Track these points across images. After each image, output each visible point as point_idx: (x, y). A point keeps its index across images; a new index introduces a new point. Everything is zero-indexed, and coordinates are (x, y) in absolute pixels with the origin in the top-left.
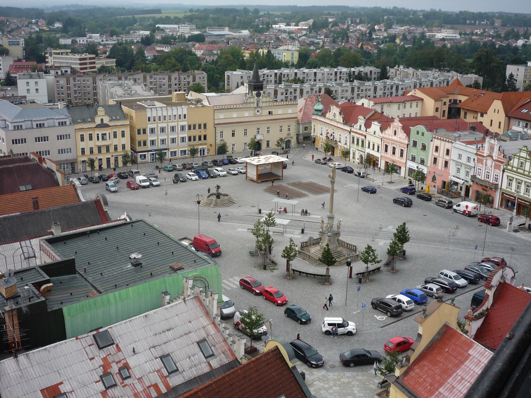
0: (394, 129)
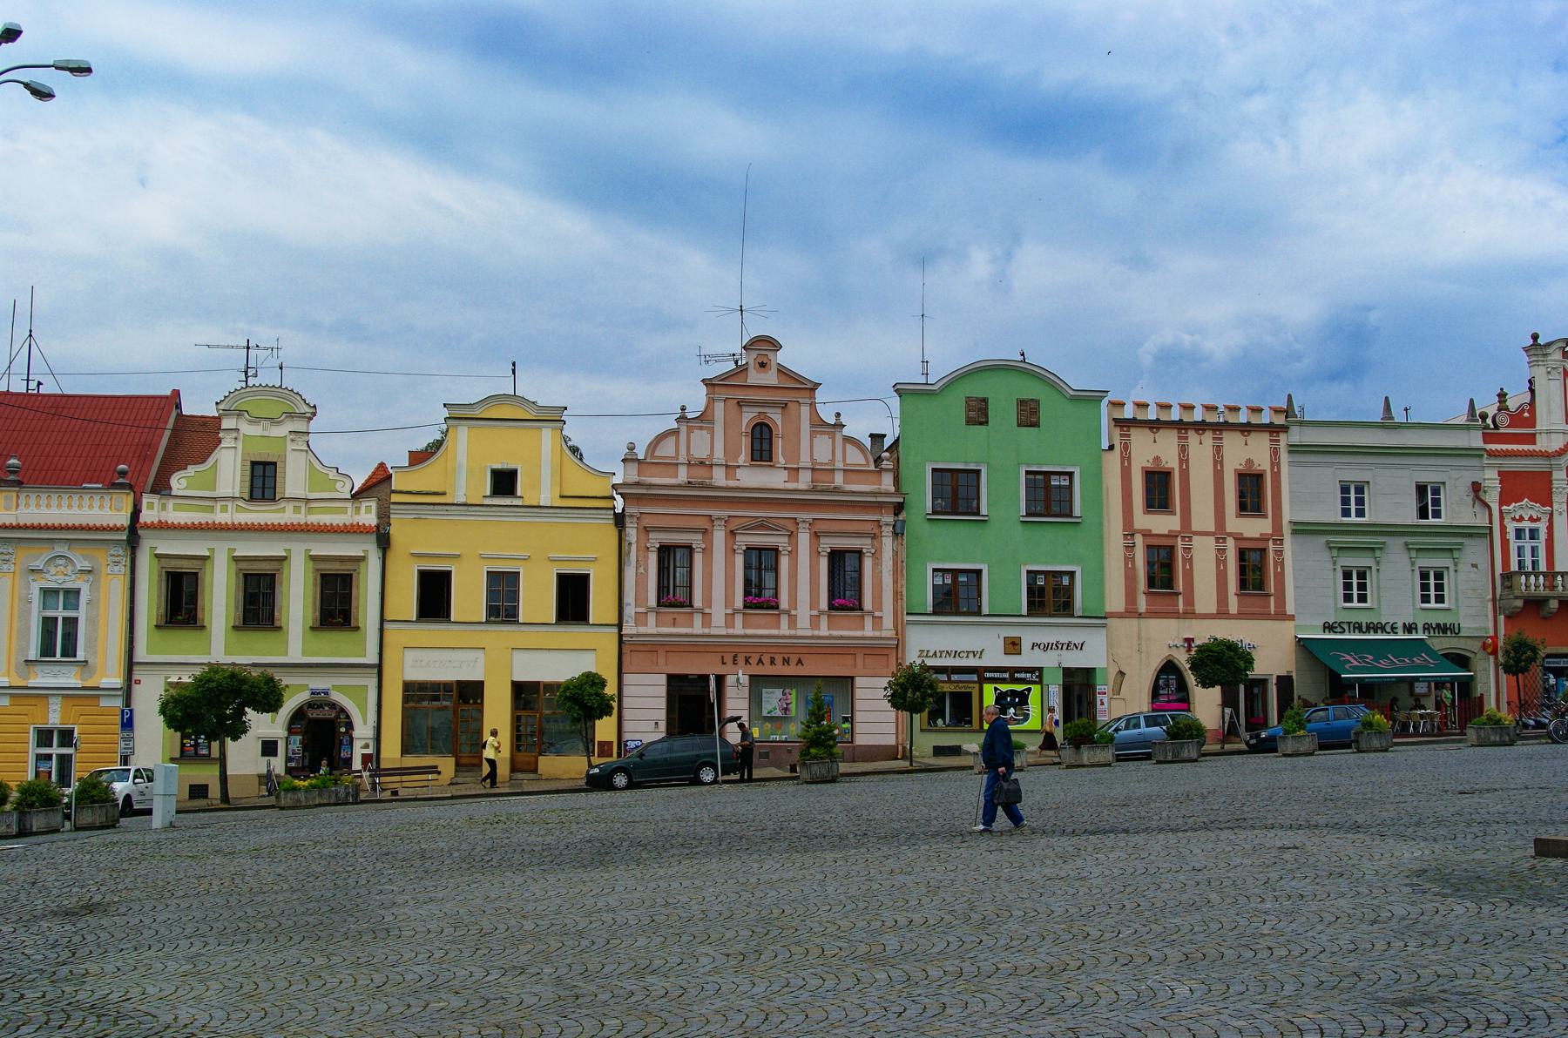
0: (749, 416)
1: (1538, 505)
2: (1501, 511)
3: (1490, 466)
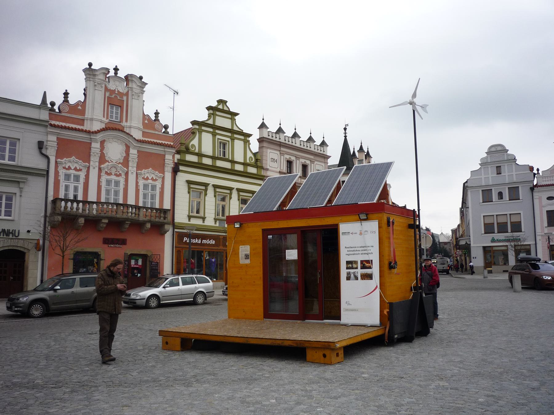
1: (81, 161)
2: (56, 162)
3: (53, 133)
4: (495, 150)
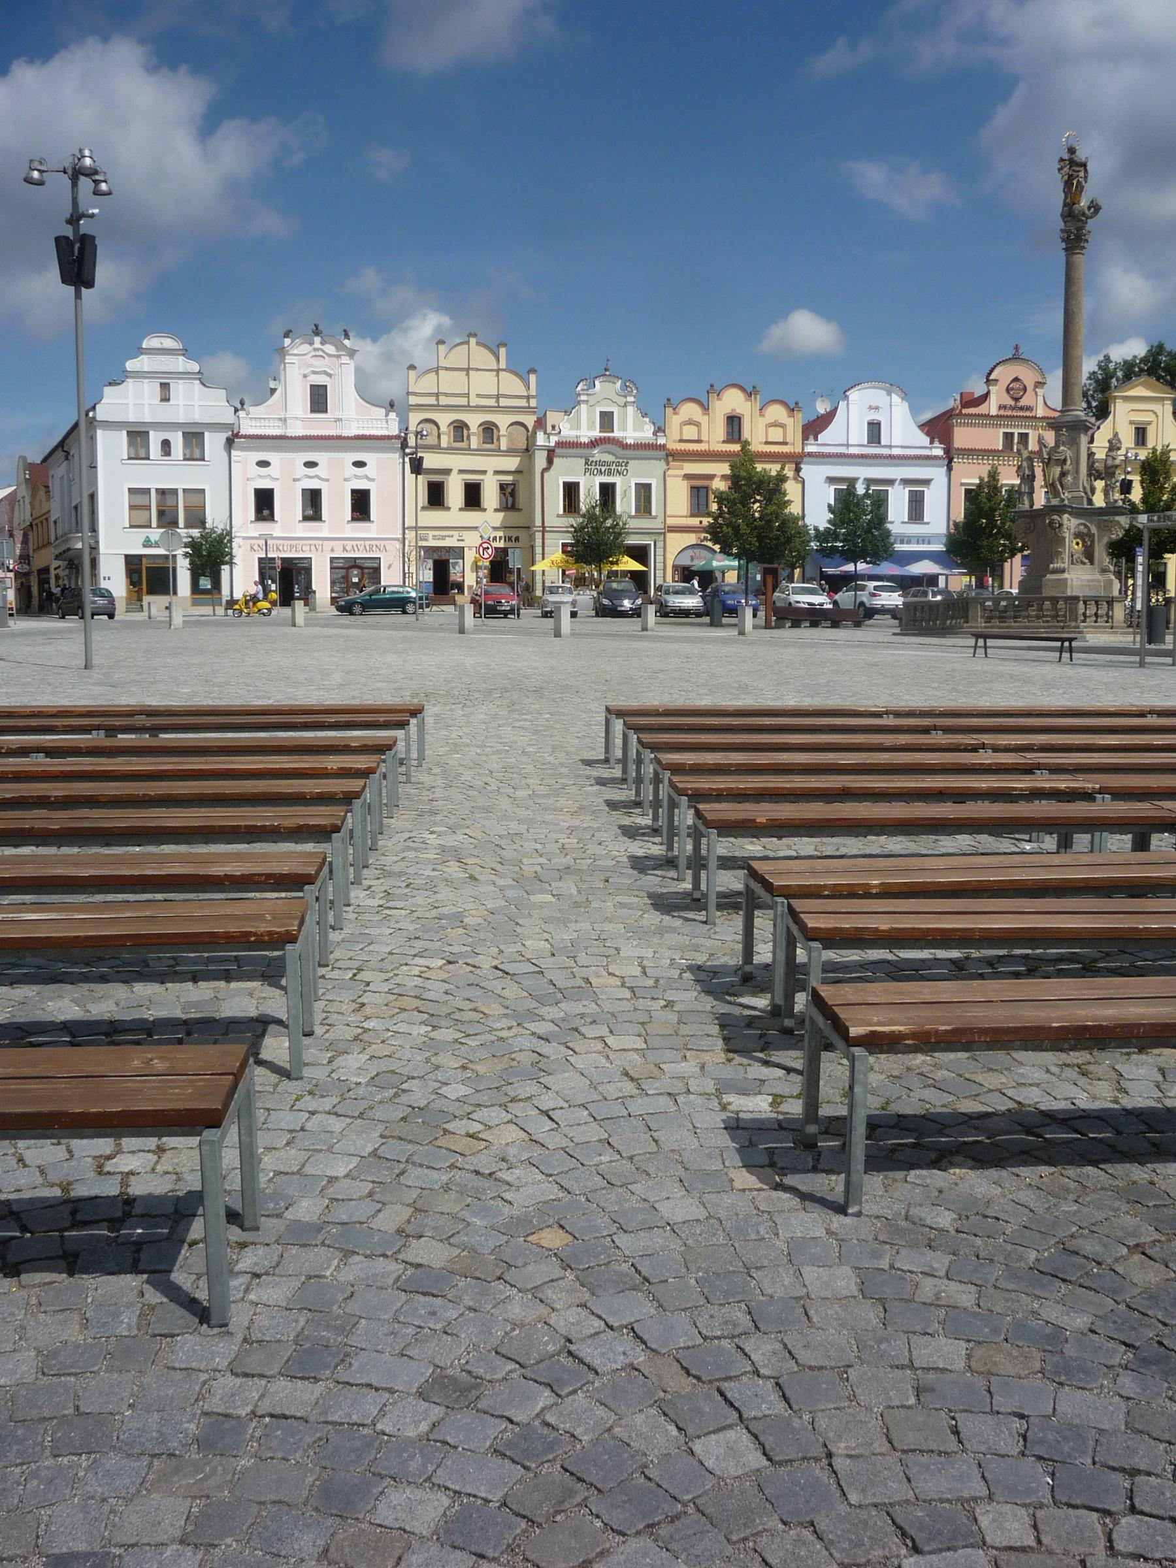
4: (159, 346)
